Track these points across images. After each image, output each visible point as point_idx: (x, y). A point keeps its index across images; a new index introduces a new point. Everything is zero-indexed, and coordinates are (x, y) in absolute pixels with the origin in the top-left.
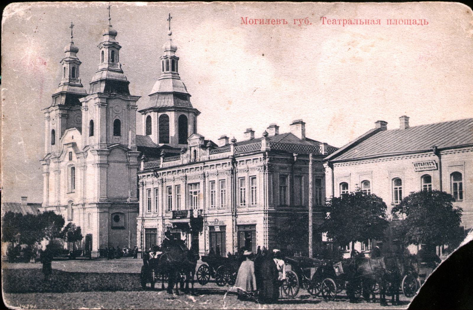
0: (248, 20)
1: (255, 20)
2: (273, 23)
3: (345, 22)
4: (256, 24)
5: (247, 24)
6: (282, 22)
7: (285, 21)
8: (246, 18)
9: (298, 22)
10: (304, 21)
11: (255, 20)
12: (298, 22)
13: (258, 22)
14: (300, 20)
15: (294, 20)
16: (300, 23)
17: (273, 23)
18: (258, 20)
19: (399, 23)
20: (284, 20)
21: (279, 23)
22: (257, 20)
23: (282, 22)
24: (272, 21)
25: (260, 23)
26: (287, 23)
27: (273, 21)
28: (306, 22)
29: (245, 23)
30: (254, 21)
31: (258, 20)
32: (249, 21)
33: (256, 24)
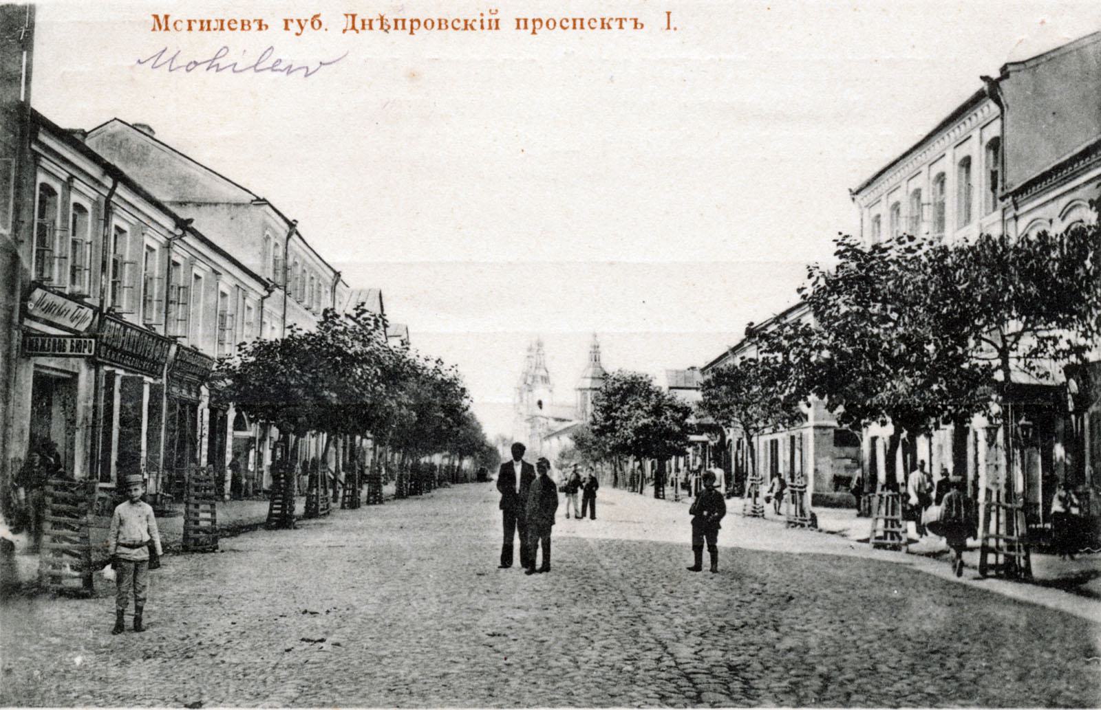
0: (171, 21)
5: (167, 29)
6: (255, 26)
7: (263, 23)
8: (166, 17)
9: (294, 27)
12: (294, 27)
13: (196, 26)
14: (299, 21)
15: (286, 21)
16: (299, 30)
18: (195, 21)
19: (433, 23)
24: (229, 24)
29: (164, 27)
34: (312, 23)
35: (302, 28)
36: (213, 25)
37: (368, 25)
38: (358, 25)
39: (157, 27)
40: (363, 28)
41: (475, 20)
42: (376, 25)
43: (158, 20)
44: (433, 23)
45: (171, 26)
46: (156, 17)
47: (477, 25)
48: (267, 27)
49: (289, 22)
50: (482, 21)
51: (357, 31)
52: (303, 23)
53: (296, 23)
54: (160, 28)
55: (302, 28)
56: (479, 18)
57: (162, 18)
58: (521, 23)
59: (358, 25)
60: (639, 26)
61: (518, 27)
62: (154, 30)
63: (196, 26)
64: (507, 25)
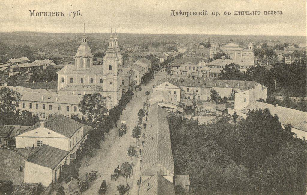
0: (35, 12)
2: (54, 15)
4: (41, 16)
5: (34, 16)
6: (60, 14)
8: (34, 11)
9: (72, 15)
10: (76, 13)
11: (41, 13)
13: (43, 15)
14: (74, 12)
15: (70, 12)
17: (54, 15)
20: (61, 12)
21: (58, 15)
22: (42, 13)
23: (60, 14)
24: (52, 14)
26: (64, 15)
27: (53, 13)
28: (78, 14)
29: (33, 15)
30: (40, 13)
32: (39, 14)
33: (41, 16)
34: (77, 13)
35: (75, 15)
36: (48, 14)
39: (31, 15)
43: (31, 13)
45: (35, 15)
46: (31, 11)
48: (64, 15)
49: (71, 13)
52: (75, 13)
53: (73, 13)
54: (32, 15)
55: (75, 15)
57: (32, 12)
62: (30, 16)
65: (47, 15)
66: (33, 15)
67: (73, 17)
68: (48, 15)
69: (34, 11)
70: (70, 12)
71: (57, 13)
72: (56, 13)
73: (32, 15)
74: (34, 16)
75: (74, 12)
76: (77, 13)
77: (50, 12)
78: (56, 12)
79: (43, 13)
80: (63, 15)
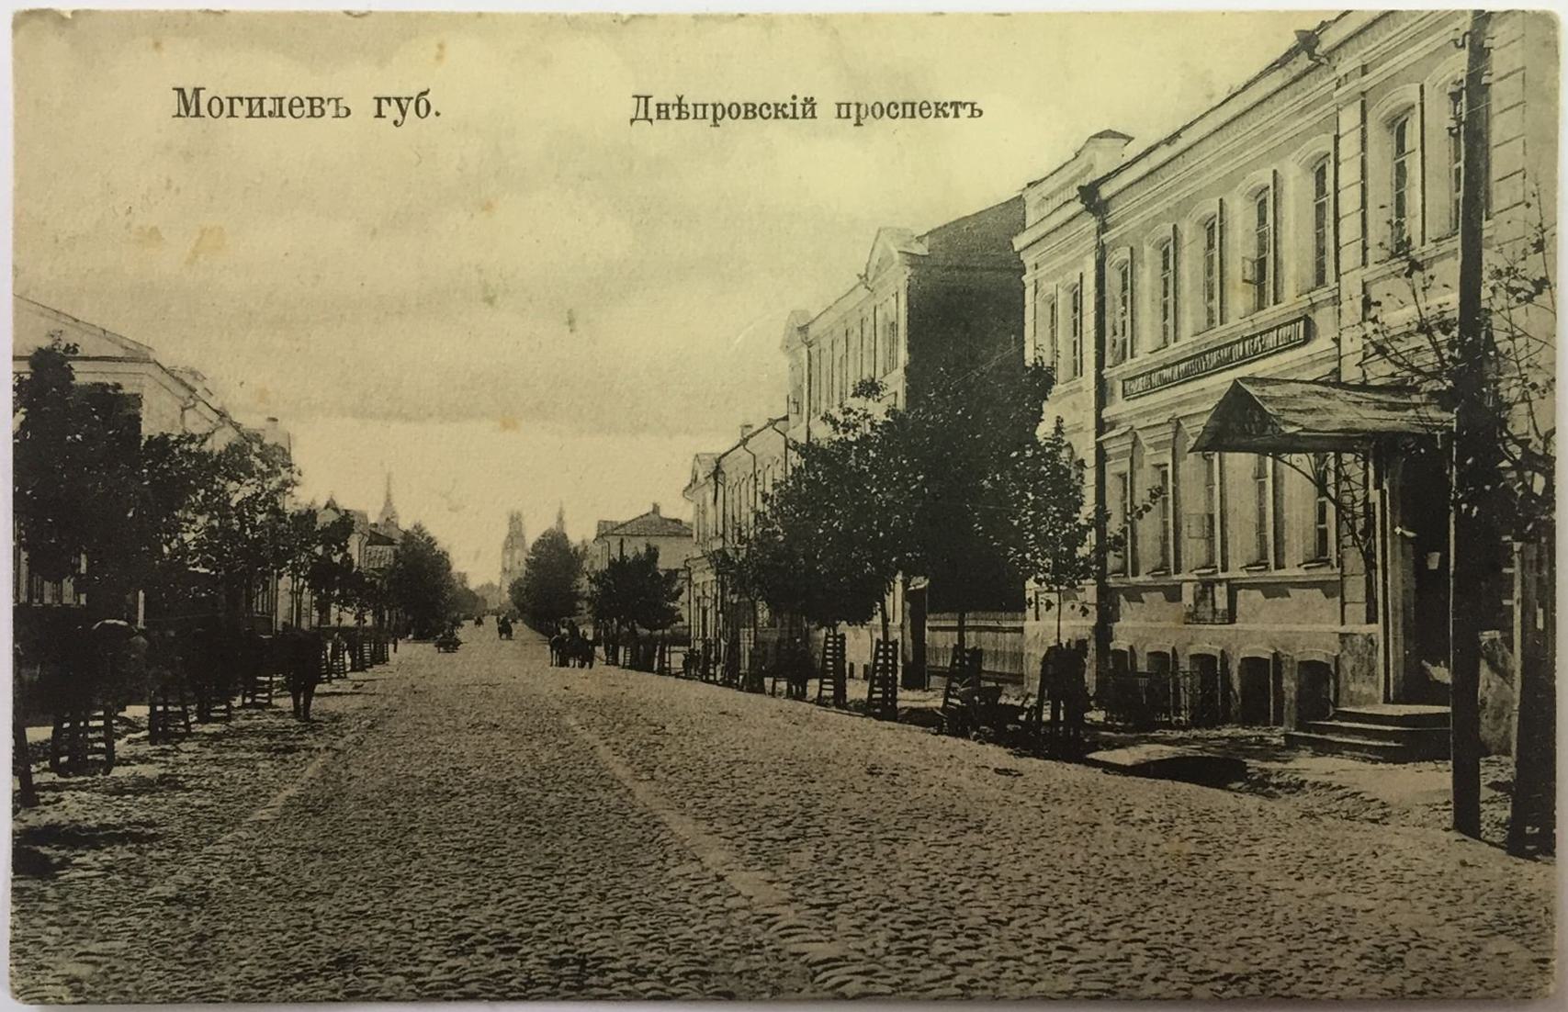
0: (204, 98)
1: (231, 99)
3: (719, 110)
4: (232, 115)
5: (197, 114)
8: (197, 91)
9: (391, 111)
10: (413, 103)
11: (231, 99)
12: (391, 111)
13: (241, 110)
14: (398, 100)
15: (379, 100)
17: (297, 112)
18: (241, 99)
19: (738, 108)
21: (317, 112)
22: (236, 102)
23: (330, 109)
25: (251, 115)
26: (348, 113)
27: (296, 102)
29: (192, 112)
30: (226, 103)
31: (241, 99)
33: (232, 115)
34: (417, 102)
35: (404, 113)
36: (268, 105)
37: (663, 111)
38: (653, 113)
39: (183, 112)
40: (659, 117)
41: (785, 106)
42: (674, 113)
43: (184, 98)
44: (738, 108)
46: (181, 91)
47: (789, 111)
48: (348, 113)
50: (794, 105)
51: (651, 120)
52: (404, 102)
53: (394, 102)
54: (187, 110)
55: (404, 113)
56: (789, 101)
57: (189, 94)
58: (843, 110)
59: (653, 113)
60: (976, 113)
61: (839, 116)
62: (179, 115)
63: (241, 110)
64: (825, 109)
65: (266, 113)
66: (192, 112)
67: (395, 122)
68: (270, 113)
69: (197, 91)
70: (379, 100)
71: (317, 102)
72: (307, 103)
73: (187, 110)
74: (197, 114)
75: (398, 100)
76: (417, 102)
77: (281, 99)
78: (312, 99)
79: (246, 102)
80: (342, 112)
